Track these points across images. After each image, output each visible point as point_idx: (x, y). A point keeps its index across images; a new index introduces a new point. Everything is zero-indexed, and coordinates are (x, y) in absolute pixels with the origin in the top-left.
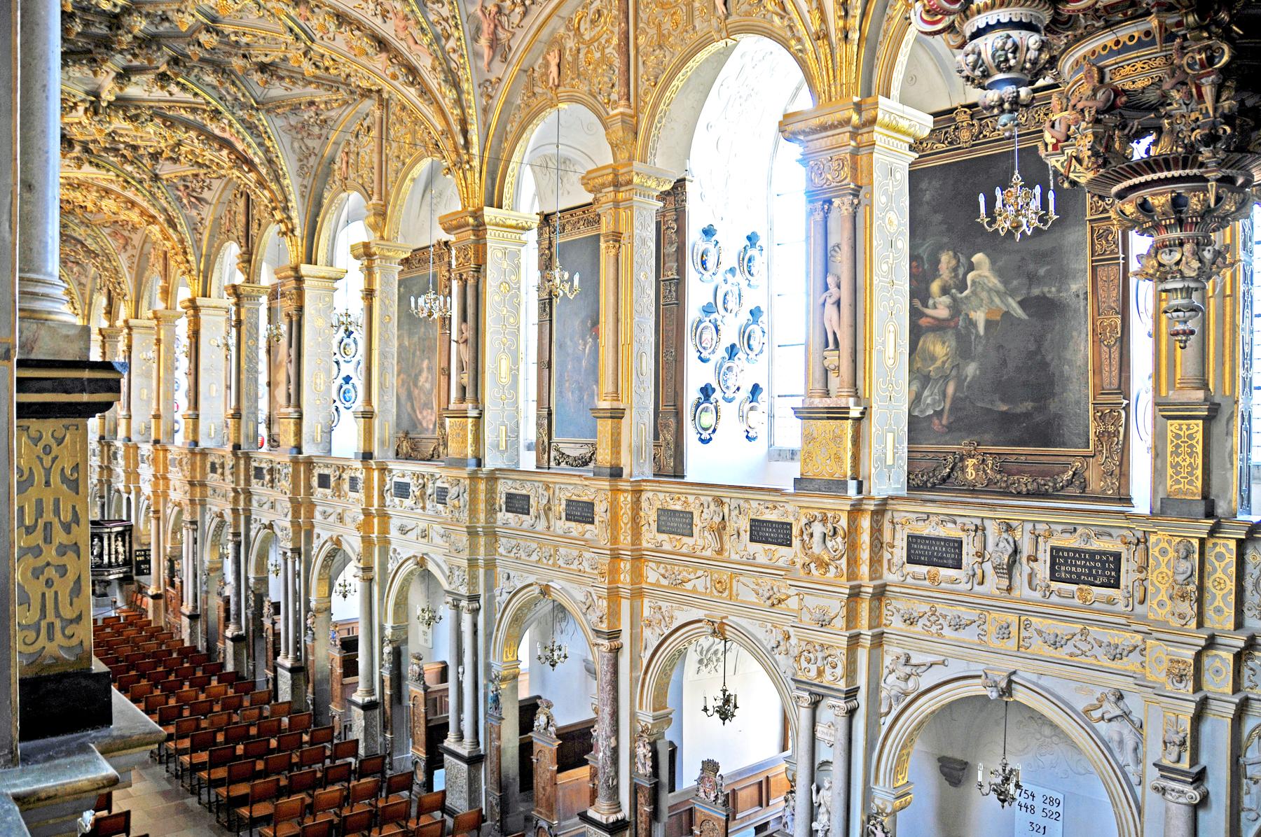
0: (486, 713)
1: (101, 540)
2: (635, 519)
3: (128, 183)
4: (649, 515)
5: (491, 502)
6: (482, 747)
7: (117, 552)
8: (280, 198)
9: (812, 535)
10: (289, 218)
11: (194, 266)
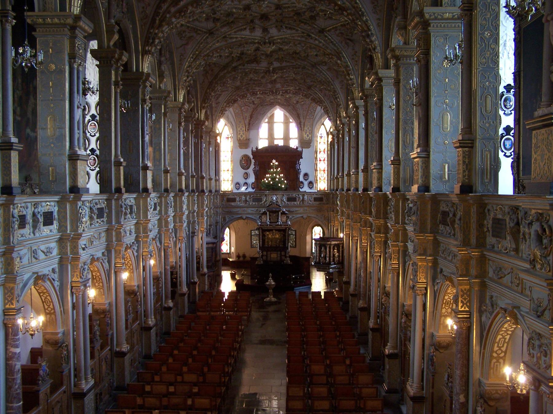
0: (428, 368)
1: (326, 249)
2: (480, 226)
3: (309, 36)
4: (488, 223)
5: (434, 217)
6: (424, 392)
7: (334, 255)
8: (366, 29)
9: (530, 234)
10: (371, 41)
11: (355, 81)
